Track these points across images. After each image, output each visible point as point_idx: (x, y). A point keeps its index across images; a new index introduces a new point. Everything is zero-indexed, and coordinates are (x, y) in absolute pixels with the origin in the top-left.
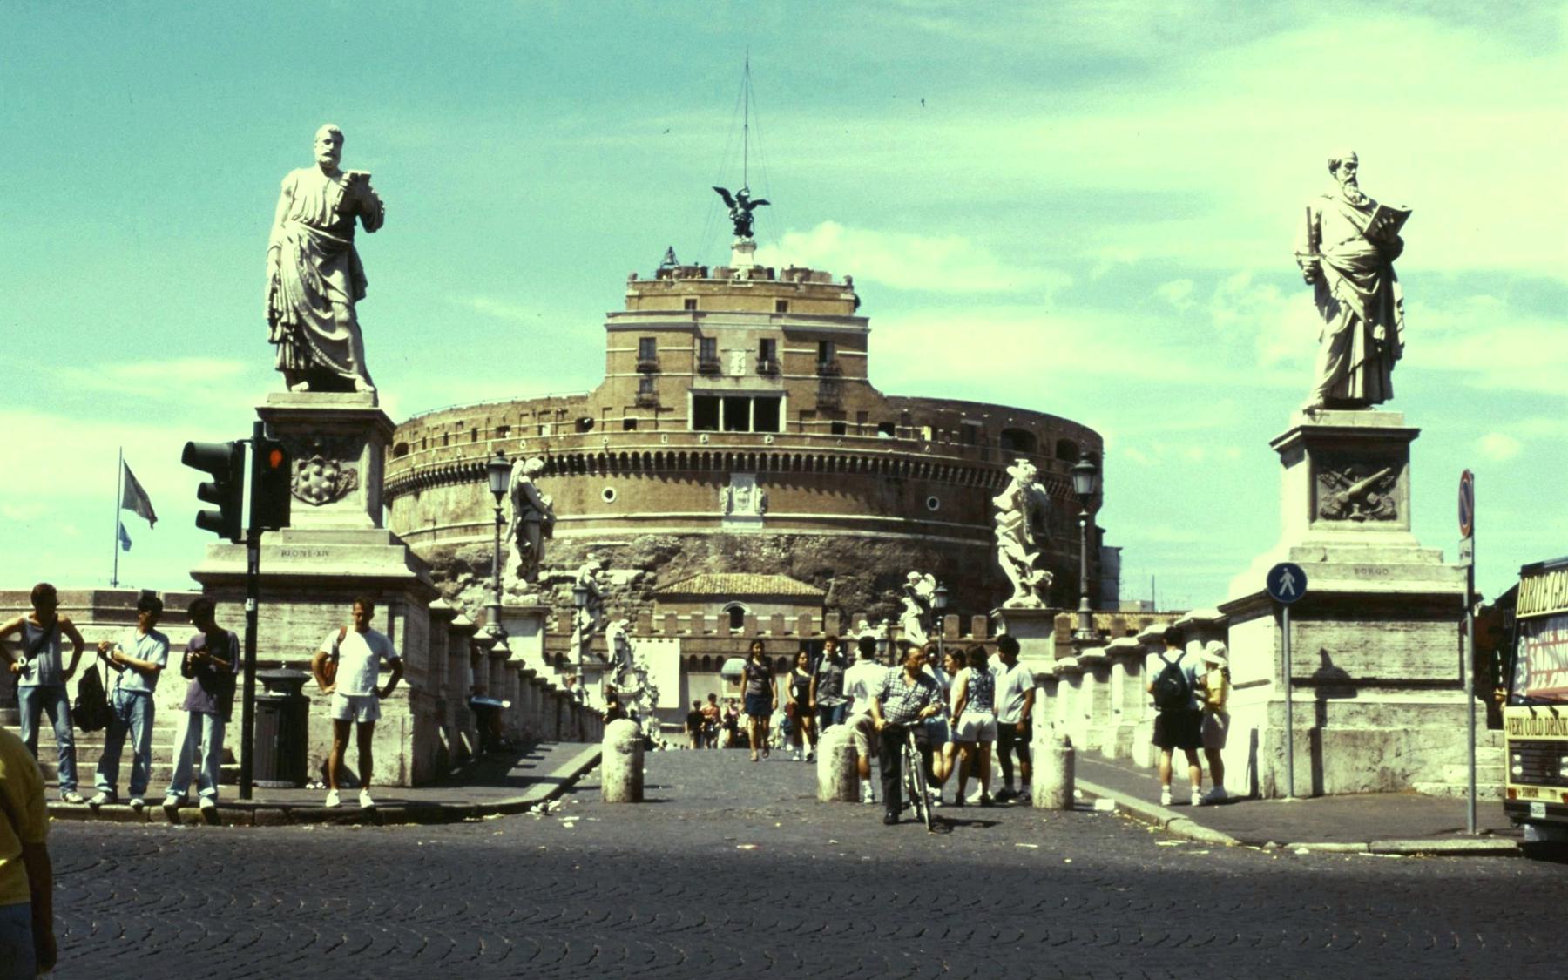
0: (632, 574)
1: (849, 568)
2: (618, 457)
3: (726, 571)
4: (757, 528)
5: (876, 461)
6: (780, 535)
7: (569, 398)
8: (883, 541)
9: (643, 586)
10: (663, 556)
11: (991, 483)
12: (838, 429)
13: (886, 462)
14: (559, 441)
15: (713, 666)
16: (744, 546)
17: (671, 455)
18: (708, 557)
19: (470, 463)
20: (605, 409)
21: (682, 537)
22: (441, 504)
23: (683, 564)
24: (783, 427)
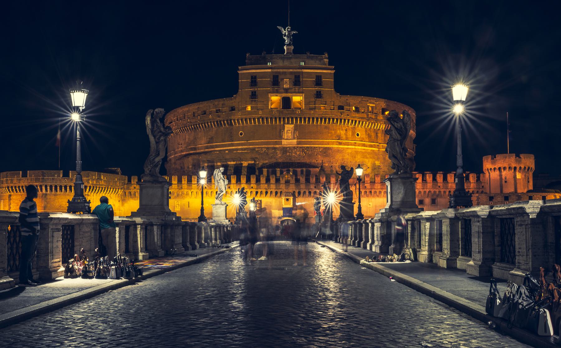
0: (250, 162)
6: (303, 147)
11: (378, 127)
15: (279, 194)
18: (277, 155)
19: (192, 124)
21: (268, 148)
22: (184, 140)
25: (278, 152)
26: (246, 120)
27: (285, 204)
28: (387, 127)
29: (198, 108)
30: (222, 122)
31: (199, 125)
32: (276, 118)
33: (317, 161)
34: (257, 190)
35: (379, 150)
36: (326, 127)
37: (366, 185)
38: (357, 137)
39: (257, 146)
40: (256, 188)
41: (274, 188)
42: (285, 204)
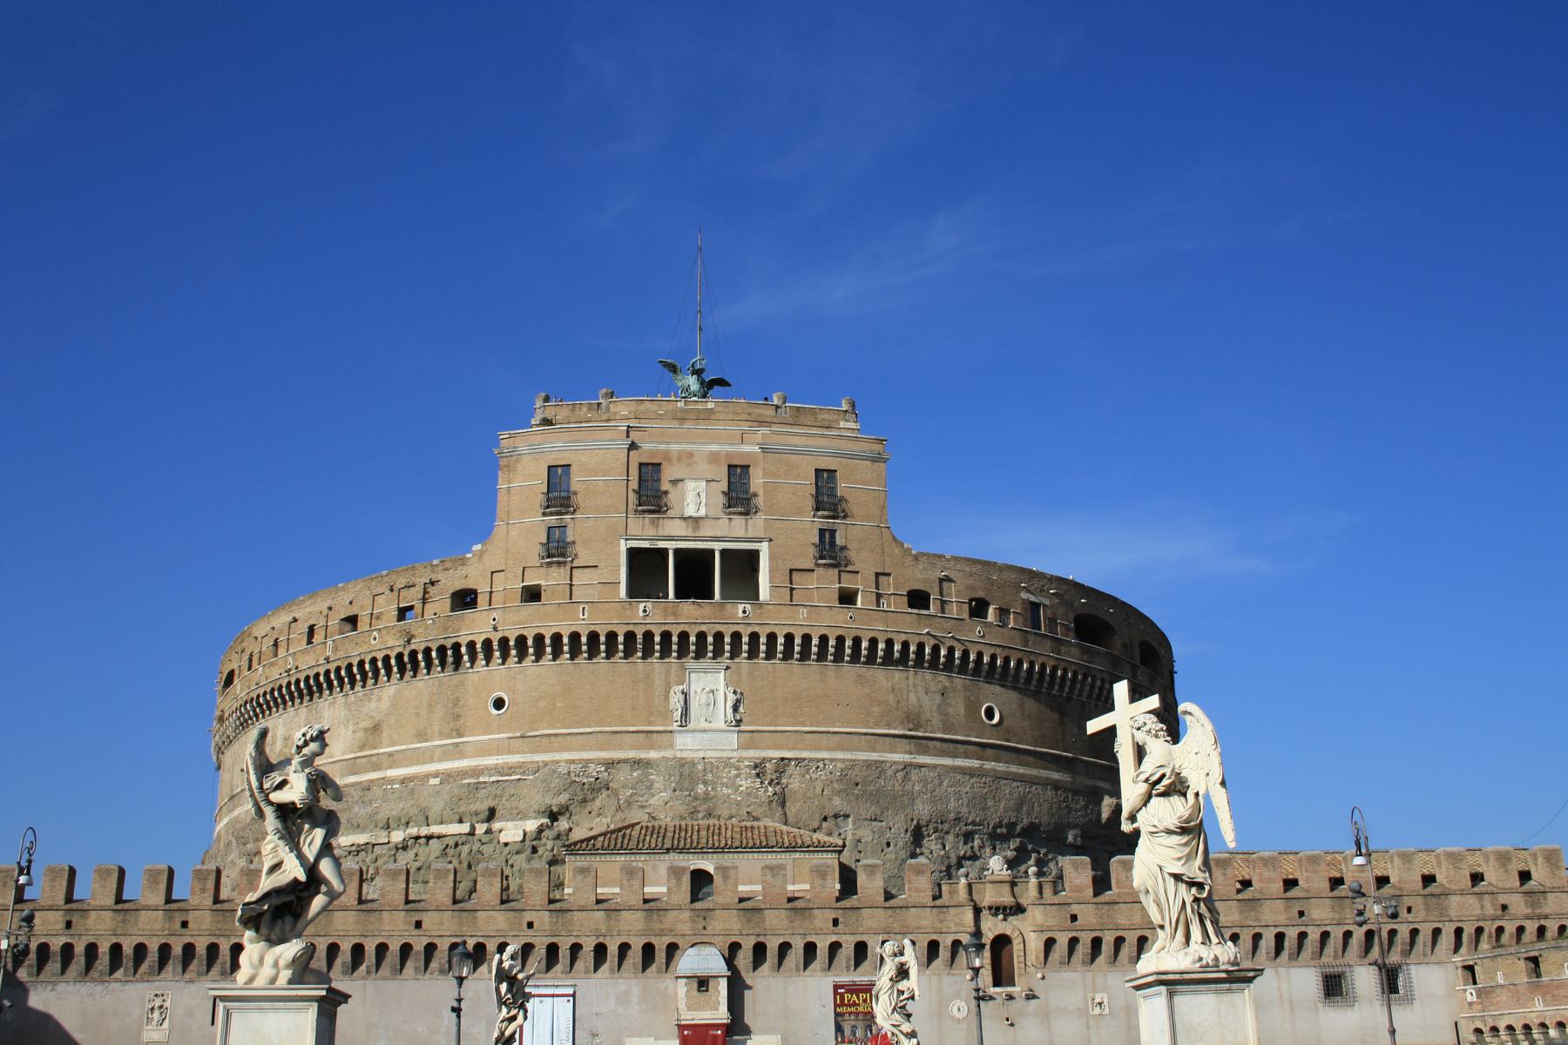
0: (532, 825)
1: (874, 810)
2: (512, 643)
3: (682, 818)
4: (727, 744)
5: (905, 645)
6: (764, 759)
7: (443, 562)
8: (921, 766)
9: (550, 844)
10: (587, 791)
12: (847, 598)
13: (921, 646)
14: (427, 628)
15: (660, 956)
16: (709, 777)
17: (594, 637)
18: (653, 796)
19: (302, 677)
20: (492, 573)
21: (610, 764)
23: (614, 808)
24: (764, 592)
25: (657, 779)
26: (521, 640)
27: (690, 1008)
28: (1097, 690)
29: (330, 609)
30: (420, 657)
31: (327, 673)
32: (649, 636)
33: (825, 819)
34: (554, 940)
35: (1072, 783)
36: (860, 679)
37: (1075, 909)
38: (990, 722)
39: (566, 756)
40: (547, 927)
41: (640, 925)
42: (690, 1008)
